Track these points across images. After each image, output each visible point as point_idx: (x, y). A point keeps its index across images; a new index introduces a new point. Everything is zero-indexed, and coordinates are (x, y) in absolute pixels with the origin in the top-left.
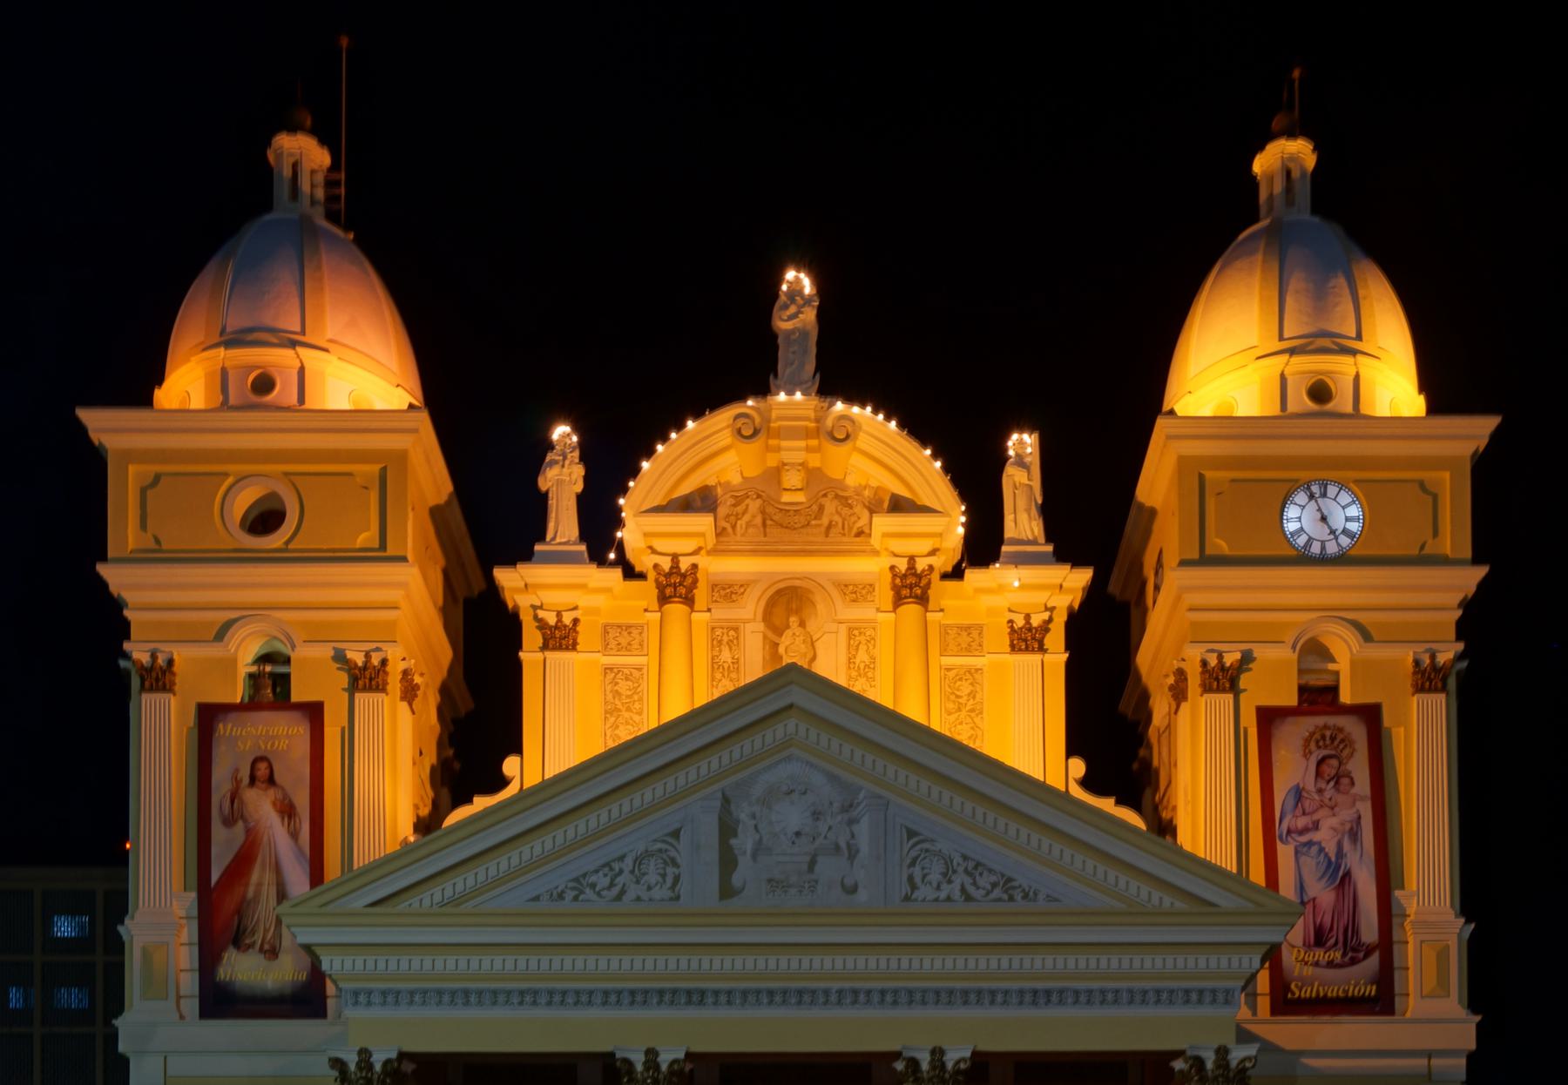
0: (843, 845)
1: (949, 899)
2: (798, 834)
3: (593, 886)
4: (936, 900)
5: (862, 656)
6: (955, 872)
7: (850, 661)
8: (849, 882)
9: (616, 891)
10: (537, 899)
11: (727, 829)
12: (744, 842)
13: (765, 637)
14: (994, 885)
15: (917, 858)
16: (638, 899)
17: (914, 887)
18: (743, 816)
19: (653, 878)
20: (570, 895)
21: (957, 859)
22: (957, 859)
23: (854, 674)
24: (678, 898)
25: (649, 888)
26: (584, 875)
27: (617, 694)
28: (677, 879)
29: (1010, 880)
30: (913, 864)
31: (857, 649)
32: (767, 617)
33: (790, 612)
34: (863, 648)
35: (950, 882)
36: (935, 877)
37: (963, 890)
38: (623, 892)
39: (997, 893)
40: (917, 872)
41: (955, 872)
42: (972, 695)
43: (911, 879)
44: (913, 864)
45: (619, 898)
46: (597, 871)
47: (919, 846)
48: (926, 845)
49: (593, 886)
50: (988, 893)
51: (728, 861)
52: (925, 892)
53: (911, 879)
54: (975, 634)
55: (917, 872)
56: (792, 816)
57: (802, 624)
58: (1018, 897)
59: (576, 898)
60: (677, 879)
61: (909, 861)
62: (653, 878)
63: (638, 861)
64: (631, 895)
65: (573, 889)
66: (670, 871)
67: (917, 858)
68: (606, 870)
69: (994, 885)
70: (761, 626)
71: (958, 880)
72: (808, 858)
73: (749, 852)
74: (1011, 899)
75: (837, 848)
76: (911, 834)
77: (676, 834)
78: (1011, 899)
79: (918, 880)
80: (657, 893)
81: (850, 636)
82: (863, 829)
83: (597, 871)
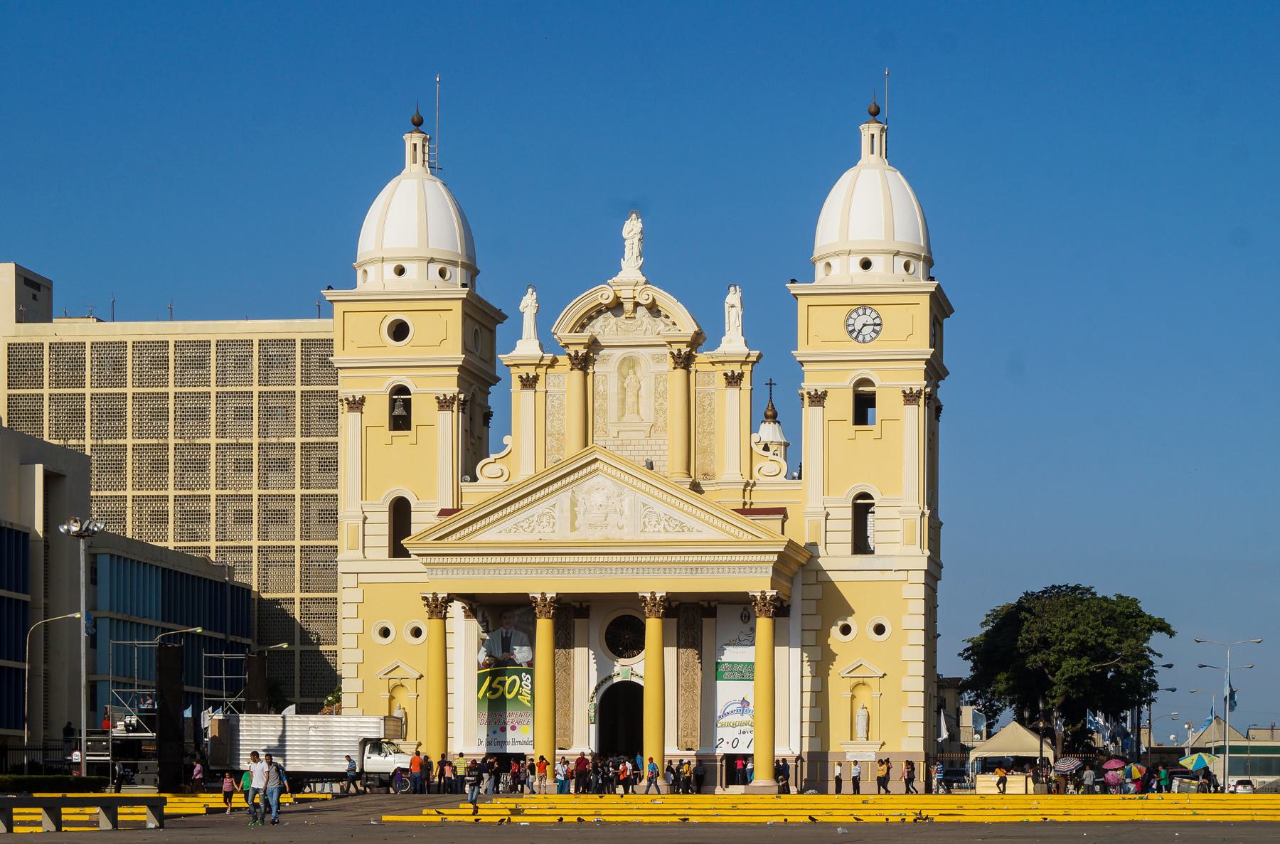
0: (618, 510)
1: (659, 531)
2: (601, 505)
3: (522, 527)
4: (654, 531)
5: (661, 388)
6: (661, 520)
7: (656, 390)
8: (620, 525)
9: (531, 528)
10: (501, 532)
11: (574, 504)
12: (580, 509)
13: (618, 380)
14: (676, 526)
15: (646, 516)
16: (540, 532)
17: (645, 526)
18: (580, 499)
19: (545, 523)
20: (514, 530)
21: (662, 515)
22: (662, 515)
23: (658, 396)
24: (554, 532)
25: (544, 528)
26: (518, 523)
27: (553, 406)
28: (554, 524)
29: (683, 523)
30: (645, 517)
31: (659, 384)
32: (619, 369)
33: (630, 368)
34: (662, 383)
35: (659, 524)
36: (653, 523)
37: (664, 528)
38: (533, 529)
39: (678, 528)
40: (647, 520)
41: (661, 520)
42: (710, 405)
43: (644, 523)
44: (645, 517)
45: (532, 532)
46: (523, 521)
47: (649, 510)
48: (651, 510)
49: (522, 527)
50: (674, 528)
51: (574, 516)
52: (649, 528)
53: (644, 523)
54: (711, 376)
55: (647, 520)
56: (598, 498)
57: (635, 373)
58: (686, 530)
59: (515, 532)
60: (554, 524)
61: (642, 518)
62: (545, 523)
63: (539, 517)
64: (537, 530)
65: (515, 528)
66: (552, 520)
67: (646, 516)
68: (527, 521)
69: (676, 526)
70: (616, 374)
71: (662, 523)
72: (604, 515)
73: (582, 510)
74: (683, 531)
75: (616, 511)
76: (644, 505)
77: (554, 506)
78: (683, 531)
79: (647, 523)
80: (547, 529)
81: (656, 375)
82: (626, 503)
83: (523, 521)
